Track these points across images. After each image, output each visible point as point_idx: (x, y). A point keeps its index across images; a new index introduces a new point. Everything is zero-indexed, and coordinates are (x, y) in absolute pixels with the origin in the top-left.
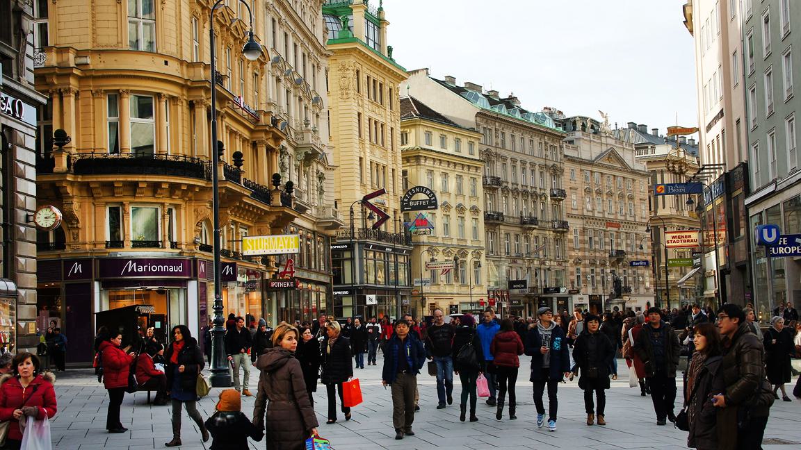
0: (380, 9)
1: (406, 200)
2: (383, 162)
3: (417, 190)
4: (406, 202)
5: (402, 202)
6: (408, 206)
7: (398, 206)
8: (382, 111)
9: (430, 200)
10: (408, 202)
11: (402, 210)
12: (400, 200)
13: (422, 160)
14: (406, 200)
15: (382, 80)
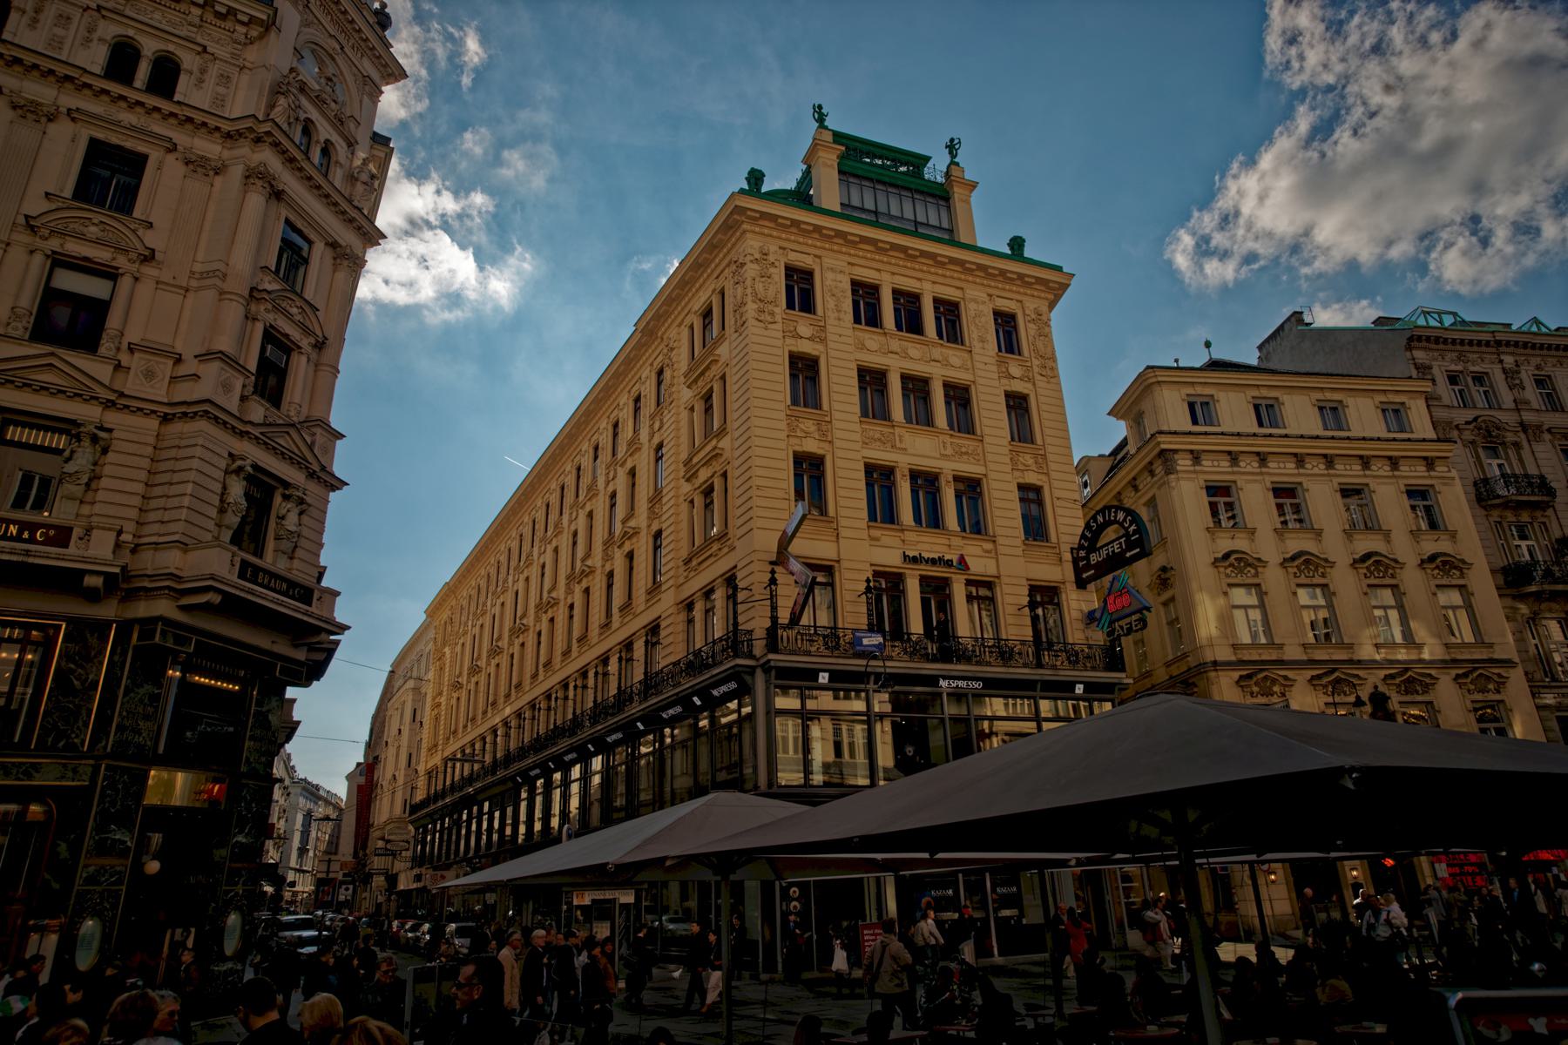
0: (952, 163)
1: (1082, 554)
2: (948, 468)
3: (1100, 519)
4: (1083, 559)
5: (1075, 561)
6: (1088, 567)
7: (1057, 572)
8: (954, 355)
9: (1127, 535)
10: (1087, 558)
11: (1081, 584)
12: (1068, 556)
13: (1184, 463)
14: (1082, 554)
15: (949, 293)
